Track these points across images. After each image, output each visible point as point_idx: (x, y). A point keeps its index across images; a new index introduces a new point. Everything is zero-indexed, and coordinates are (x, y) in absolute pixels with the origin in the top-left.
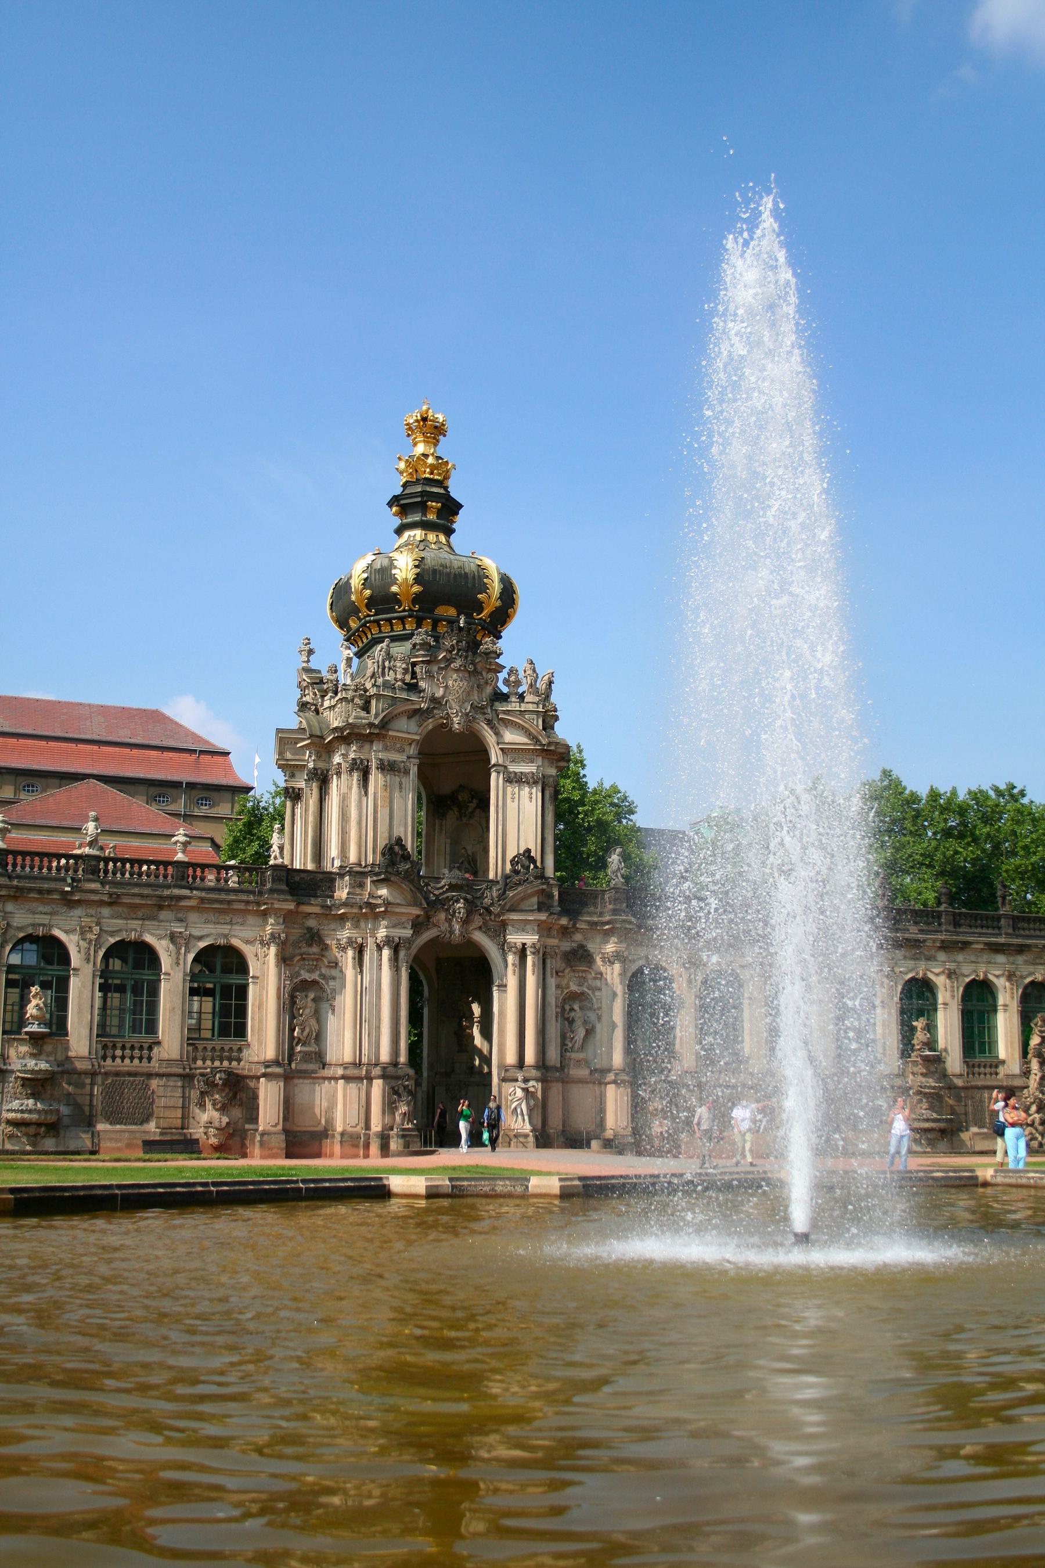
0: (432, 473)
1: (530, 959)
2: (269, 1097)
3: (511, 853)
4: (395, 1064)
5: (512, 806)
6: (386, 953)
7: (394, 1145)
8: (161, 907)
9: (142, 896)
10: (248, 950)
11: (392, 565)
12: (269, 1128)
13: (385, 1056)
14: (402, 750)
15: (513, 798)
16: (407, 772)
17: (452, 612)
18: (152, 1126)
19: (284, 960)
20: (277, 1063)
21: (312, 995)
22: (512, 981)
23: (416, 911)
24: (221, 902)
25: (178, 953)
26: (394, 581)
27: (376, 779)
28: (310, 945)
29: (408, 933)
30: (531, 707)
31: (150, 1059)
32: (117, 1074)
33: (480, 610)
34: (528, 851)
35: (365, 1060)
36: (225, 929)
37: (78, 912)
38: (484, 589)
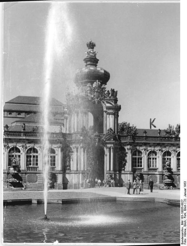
1: (111, 150)
2: (60, 178)
3: (108, 128)
5: (108, 119)
6: (82, 149)
7: (84, 186)
10: (55, 149)
12: (60, 183)
13: (82, 169)
15: (108, 118)
19: (62, 150)
20: (61, 171)
22: (108, 154)
27: (80, 115)
31: (36, 170)
34: (111, 128)
35: (78, 170)
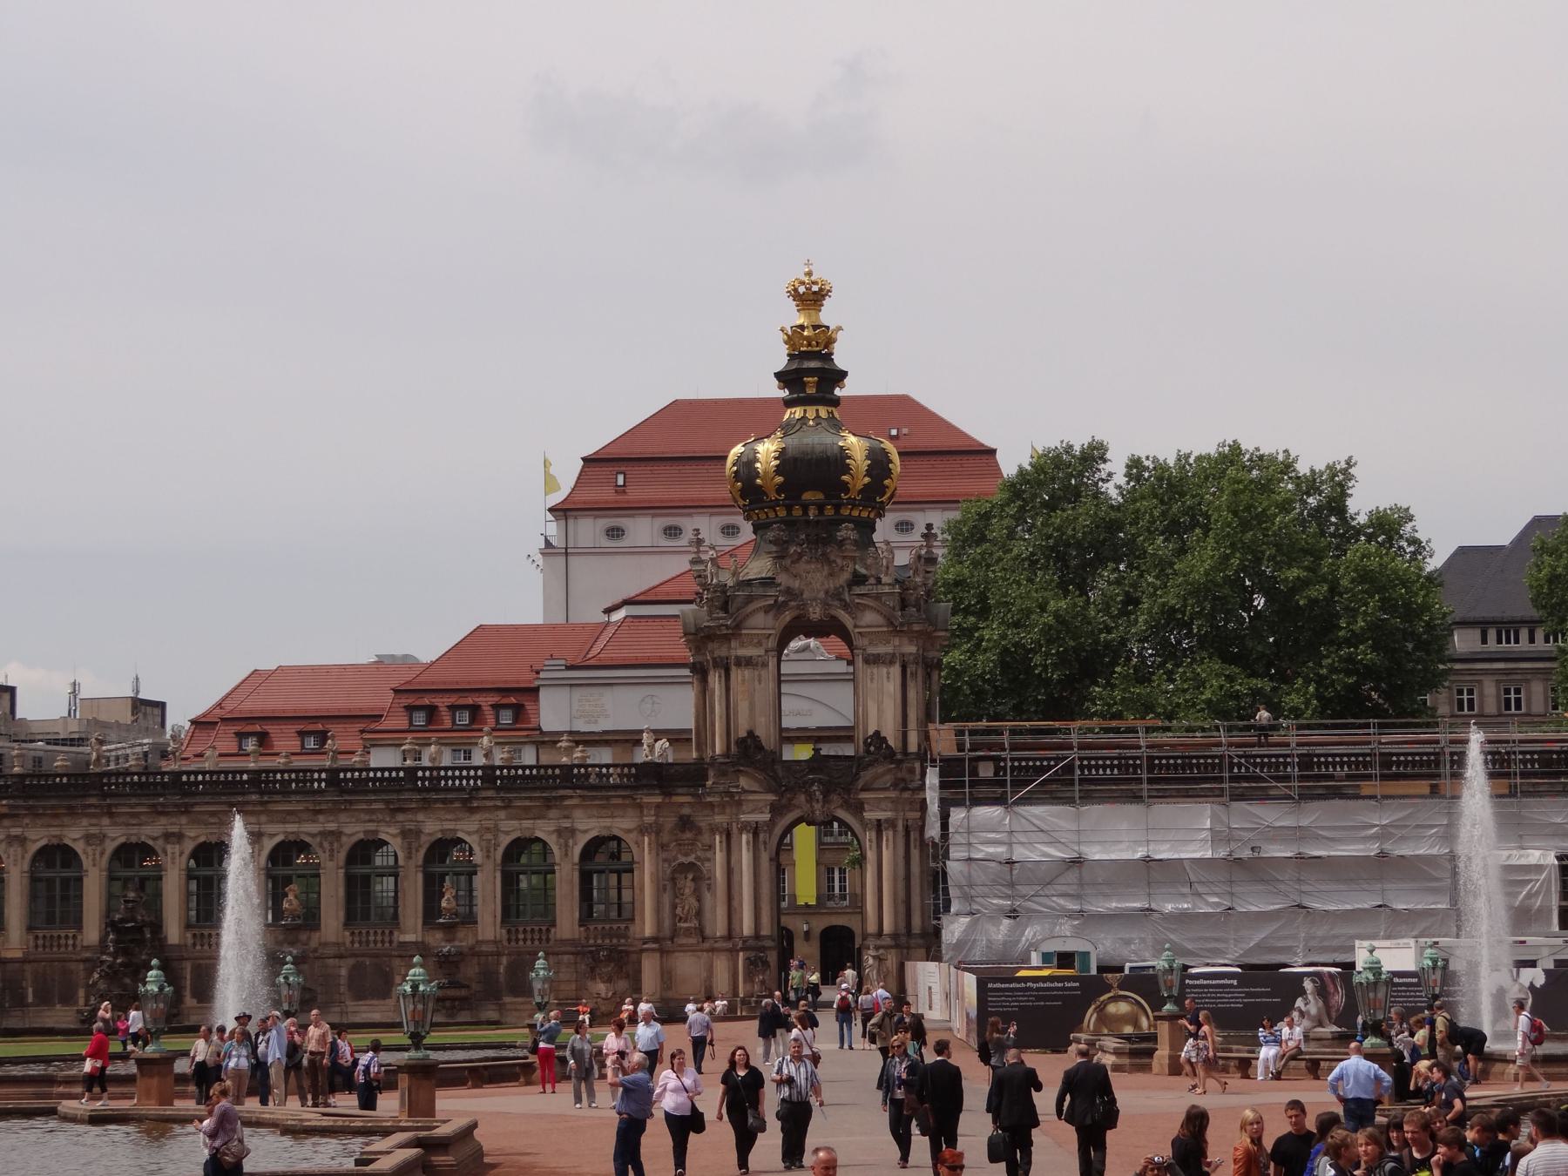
0: (809, 345)
4: (757, 936)
8: (549, 807)
9: (530, 798)
13: (747, 928)
14: (760, 644)
16: (765, 665)
17: (821, 496)
21: (690, 876)
23: (771, 797)
24: (602, 798)
25: (566, 845)
27: (737, 675)
28: (683, 831)
29: (766, 817)
30: (887, 589)
33: (847, 491)
36: (607, 822)
37: (477, 817)
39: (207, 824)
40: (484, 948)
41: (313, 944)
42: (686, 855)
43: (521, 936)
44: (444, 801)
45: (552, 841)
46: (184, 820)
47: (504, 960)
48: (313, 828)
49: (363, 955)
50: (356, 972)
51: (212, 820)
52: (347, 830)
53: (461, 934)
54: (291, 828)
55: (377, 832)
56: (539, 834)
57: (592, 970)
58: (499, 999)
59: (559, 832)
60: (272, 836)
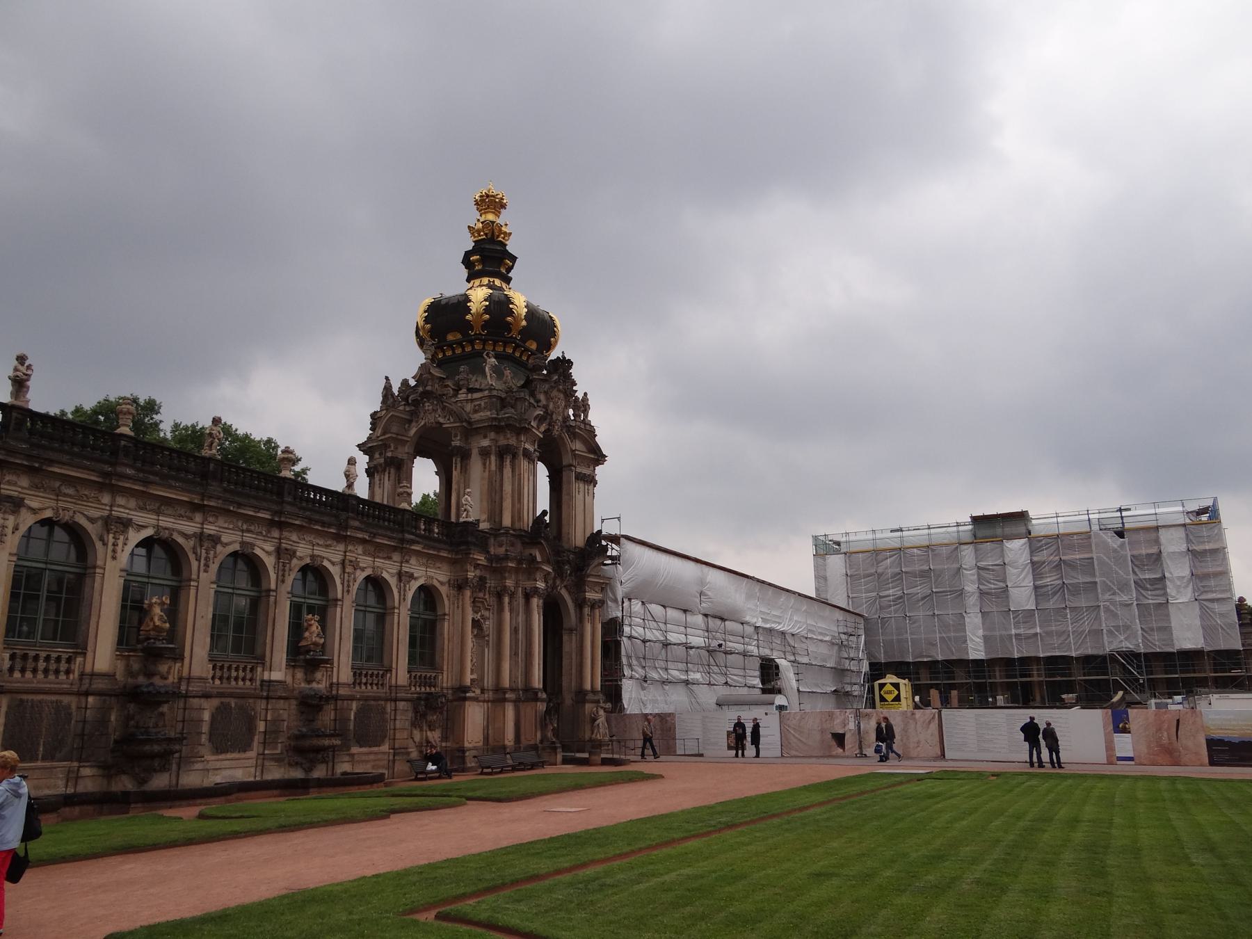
8: (395, 549)
11: (508, 300)
18: (385, 748)
24: (434, 548)
26: (511, 312)
32: (366, 699)
36: (432, 572)
37: (341, 547)
38: (554, 334)
39: (58, 494)
40: (342, 692)
41: (172, 679)
42: (476, 612)
43: (364, 680)
44: (323, 524)
45: (393, 582)
46: (24, 482)
47: (354, 705)
48: (190, 527)
49: (231, 695)
50: (221, 714)
51: (71, 491)
52: (224, 539)
53: (318, 675)
54: (166, 522)
55: (253, 545)
56: (385, 575)
57: (424, 716)
58: (349, 749)
59: (400, 575)
60: (141, 527)
